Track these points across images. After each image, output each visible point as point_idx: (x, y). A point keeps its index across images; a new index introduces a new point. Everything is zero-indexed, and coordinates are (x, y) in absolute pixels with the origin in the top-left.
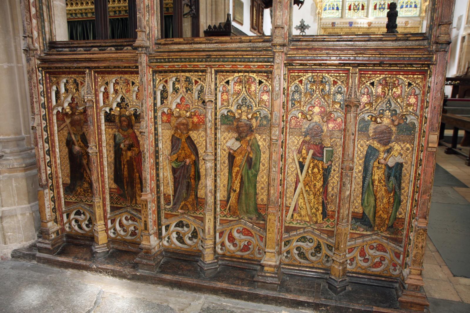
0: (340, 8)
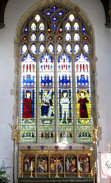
0: (35, 135)
